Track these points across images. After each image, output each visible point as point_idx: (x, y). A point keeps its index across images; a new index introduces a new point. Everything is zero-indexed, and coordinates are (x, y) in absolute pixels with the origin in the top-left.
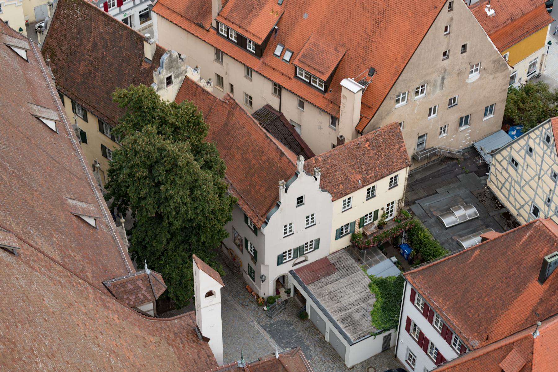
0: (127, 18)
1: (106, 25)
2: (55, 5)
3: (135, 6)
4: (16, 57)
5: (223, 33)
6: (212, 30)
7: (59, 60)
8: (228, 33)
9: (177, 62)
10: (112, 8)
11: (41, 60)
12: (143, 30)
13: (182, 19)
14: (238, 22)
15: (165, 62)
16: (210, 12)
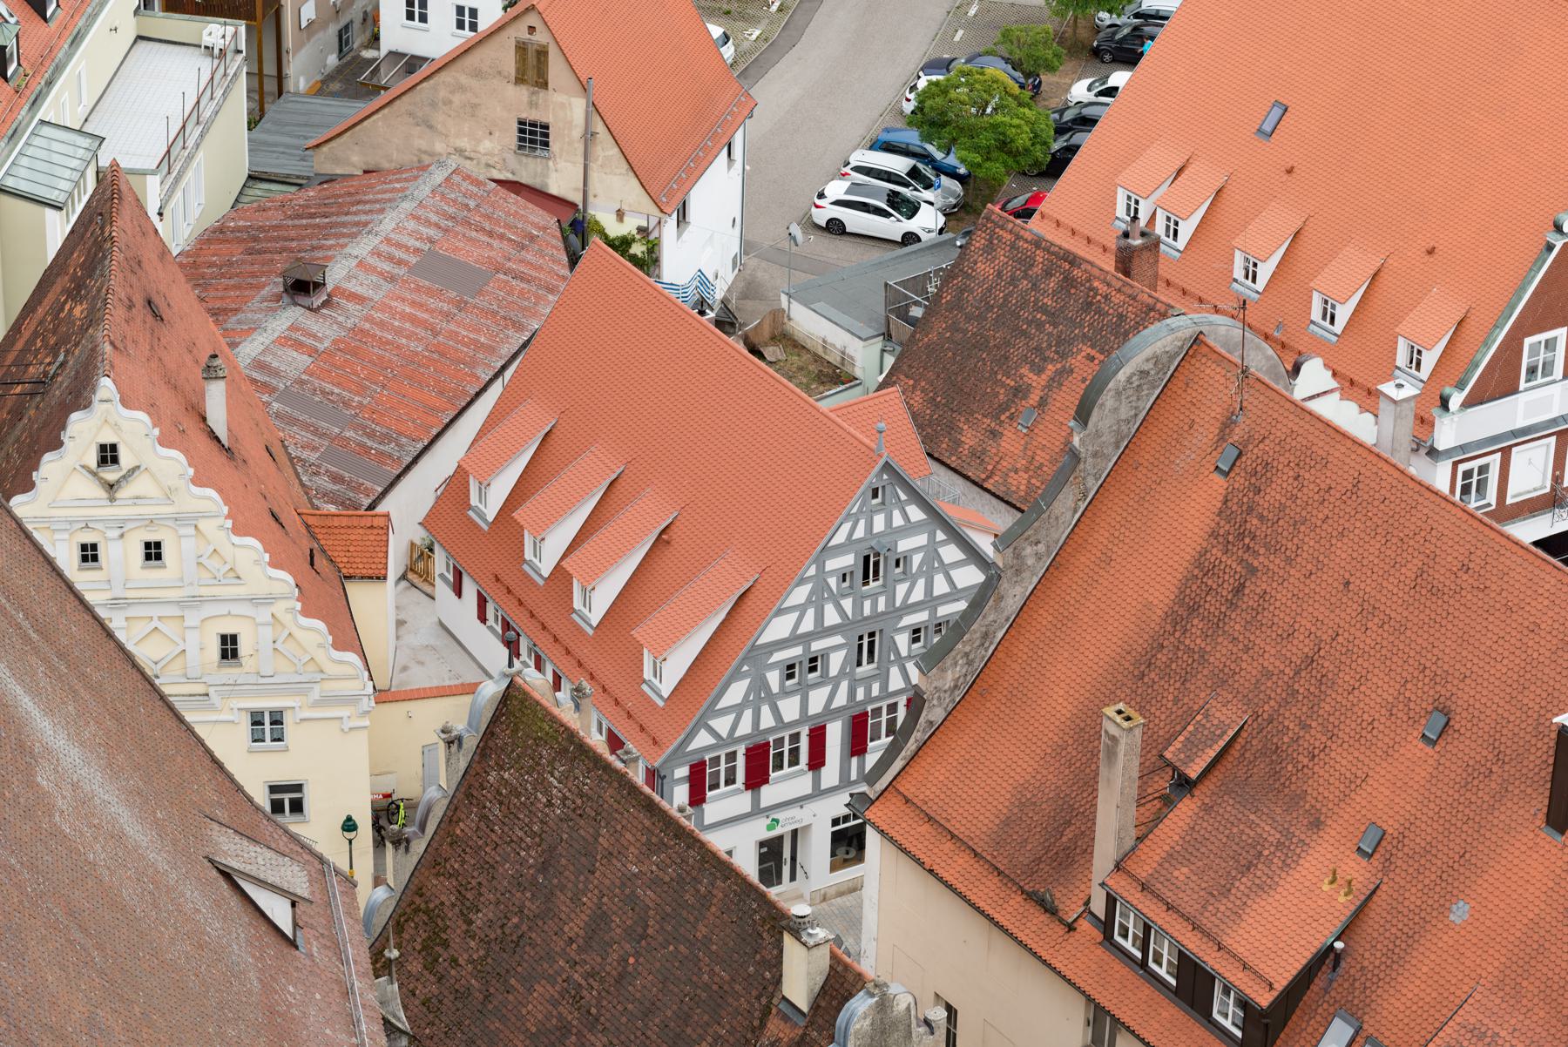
0: (780, 838)
1: (651, 848)
2: (471, 743)
3: (818, 793)
4: (246, 917)
5: (1128, 945)
6: (1085, 925)
7: (454, 961)
8: (1145, 950)
9: (909, 1034)
10: (723, 789)
11: (357, 952)
12: (840, 894)
13: (978, 869)
14: (1188, 903)
15: (855, 1027)
16: (1088, 851)
